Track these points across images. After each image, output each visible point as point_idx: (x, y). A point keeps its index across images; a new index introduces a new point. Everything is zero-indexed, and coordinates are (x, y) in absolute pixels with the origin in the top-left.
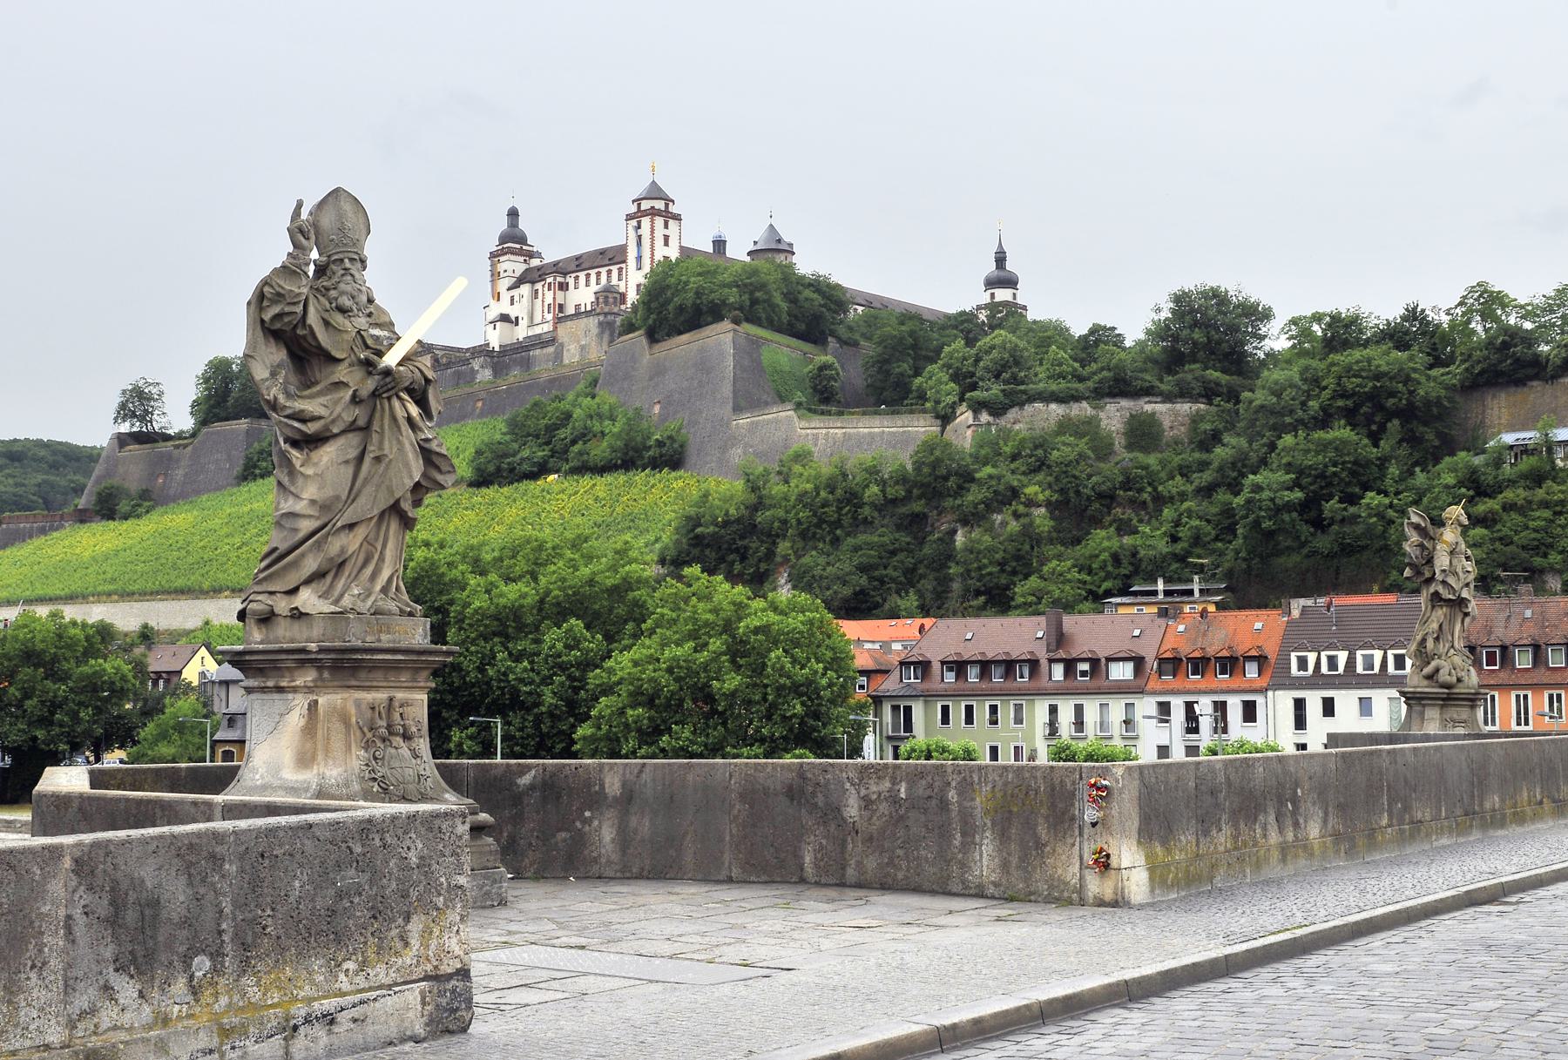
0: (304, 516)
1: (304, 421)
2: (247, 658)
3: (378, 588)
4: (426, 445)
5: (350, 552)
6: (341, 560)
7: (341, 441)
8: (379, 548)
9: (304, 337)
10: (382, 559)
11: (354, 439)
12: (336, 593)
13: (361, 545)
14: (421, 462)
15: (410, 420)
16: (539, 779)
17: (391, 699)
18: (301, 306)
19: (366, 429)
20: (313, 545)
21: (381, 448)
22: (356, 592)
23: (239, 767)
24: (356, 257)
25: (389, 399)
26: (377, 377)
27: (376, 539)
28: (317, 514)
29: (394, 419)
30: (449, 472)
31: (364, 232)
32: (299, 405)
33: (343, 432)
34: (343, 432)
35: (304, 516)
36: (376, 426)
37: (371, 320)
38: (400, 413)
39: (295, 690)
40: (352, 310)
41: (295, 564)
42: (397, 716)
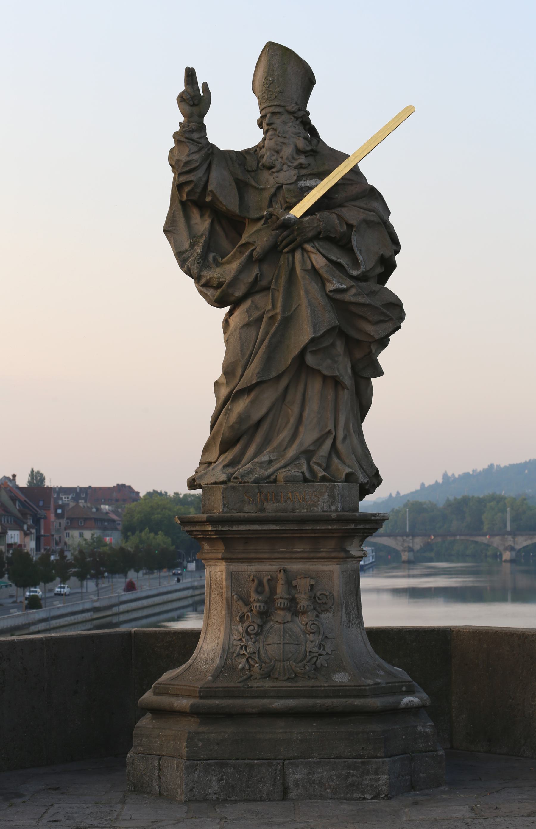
3: (291, 453)
4: (339, 296)
7: (247, 304)
15: (314, 271)
18: (200, 173)
20: (225, 414)
21: (274, 307)
24: (277, 110)
25: (293, 251)
26: (274, 233)
37: (303, 172)
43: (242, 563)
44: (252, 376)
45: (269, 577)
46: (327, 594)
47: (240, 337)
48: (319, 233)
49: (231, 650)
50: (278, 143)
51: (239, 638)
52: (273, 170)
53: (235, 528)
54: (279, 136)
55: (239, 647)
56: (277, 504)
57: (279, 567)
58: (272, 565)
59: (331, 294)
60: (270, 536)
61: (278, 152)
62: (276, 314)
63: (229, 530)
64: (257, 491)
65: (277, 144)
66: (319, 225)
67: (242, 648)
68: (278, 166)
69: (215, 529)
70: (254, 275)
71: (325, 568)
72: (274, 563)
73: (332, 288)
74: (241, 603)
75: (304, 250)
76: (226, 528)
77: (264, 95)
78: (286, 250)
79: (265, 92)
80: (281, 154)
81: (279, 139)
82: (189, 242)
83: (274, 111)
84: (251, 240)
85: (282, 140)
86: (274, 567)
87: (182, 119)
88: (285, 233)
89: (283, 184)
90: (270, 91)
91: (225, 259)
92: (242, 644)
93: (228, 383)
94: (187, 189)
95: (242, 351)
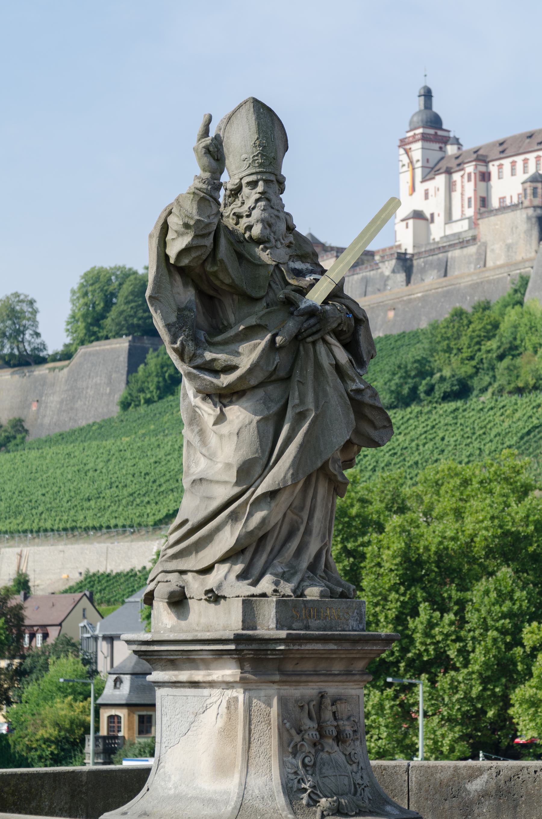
0: (218, 482)
1: (216, 373)
2: (156, 648)
3: (304, 564)
4: (359, 397)
5: (272, 524)
6: (261, 534)
7: (261, 393)
8: (305, 518)
9: (215, 274)
10: (308, 532)
11: (274, 391)
12: (256, 571)
13: (285, 515)
14: (352, 416)
15: (338, 367)
16: (493, 783)
17: (322, 696)
19: (288, 378)
21: (302, 401)
22: (280, 570)
23: (147, 772)
24: (273, 178)
25: (314, 343)
27: (302, 508)
28: (234, 479)
29: (318, 366)
30: (385, 427)
31: (281, 147)
32: (209, 356)
33: (261, 385)
34: (261, 385)
35: (218, 482)
36: (296, 377)
38: (326, 361)
39: (211, 684)
40: (268, 241)
41: (208, 539)
42: (328, 715)
43: (290, 685)
44: (285, 477)
45: (314, 703)
46: (357, 721)
47: (258, 432)
48: (339, 325)
49: (290, 785)
50: (273, 215)
51: (293, 771)
52: (267, 245)
53: (303, 647)
54: (272, 208)
55: (296, 781)
56: (318, 621)
57: (318, 691)
58: (313, 689)
59: (352, 393)
60: (323, 656)
61: (270, 225)
62: (307, 410)
63: (298, 650)
64: (303, 606)
65: (271, 217)
66: (341, 317)
67: (299, 782)
68: (273, 241)
69: (287, 648)
70: (275, 363)
71: (353, 692)
72: (315, 687)
73: (354, 387)
74: (293, 732)
75: (325, 342)
76: (296, 647)
77: (256, 158)
78: (310, 339)
79: (257, 155)
80: (274, 229)
81: (273, 211)
82: (176, 314)
83: (269, 178)
84: (262, 323)
85: (276, 213)
86: (315, 691)
87: (199, 172)
88: (312, 321)
89: (279, 263)
90: (264, 155)
91: (219, 338)
92: (299, 777)
93: (237, 484)
94: (194, 254)
95: (261, 447)
